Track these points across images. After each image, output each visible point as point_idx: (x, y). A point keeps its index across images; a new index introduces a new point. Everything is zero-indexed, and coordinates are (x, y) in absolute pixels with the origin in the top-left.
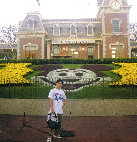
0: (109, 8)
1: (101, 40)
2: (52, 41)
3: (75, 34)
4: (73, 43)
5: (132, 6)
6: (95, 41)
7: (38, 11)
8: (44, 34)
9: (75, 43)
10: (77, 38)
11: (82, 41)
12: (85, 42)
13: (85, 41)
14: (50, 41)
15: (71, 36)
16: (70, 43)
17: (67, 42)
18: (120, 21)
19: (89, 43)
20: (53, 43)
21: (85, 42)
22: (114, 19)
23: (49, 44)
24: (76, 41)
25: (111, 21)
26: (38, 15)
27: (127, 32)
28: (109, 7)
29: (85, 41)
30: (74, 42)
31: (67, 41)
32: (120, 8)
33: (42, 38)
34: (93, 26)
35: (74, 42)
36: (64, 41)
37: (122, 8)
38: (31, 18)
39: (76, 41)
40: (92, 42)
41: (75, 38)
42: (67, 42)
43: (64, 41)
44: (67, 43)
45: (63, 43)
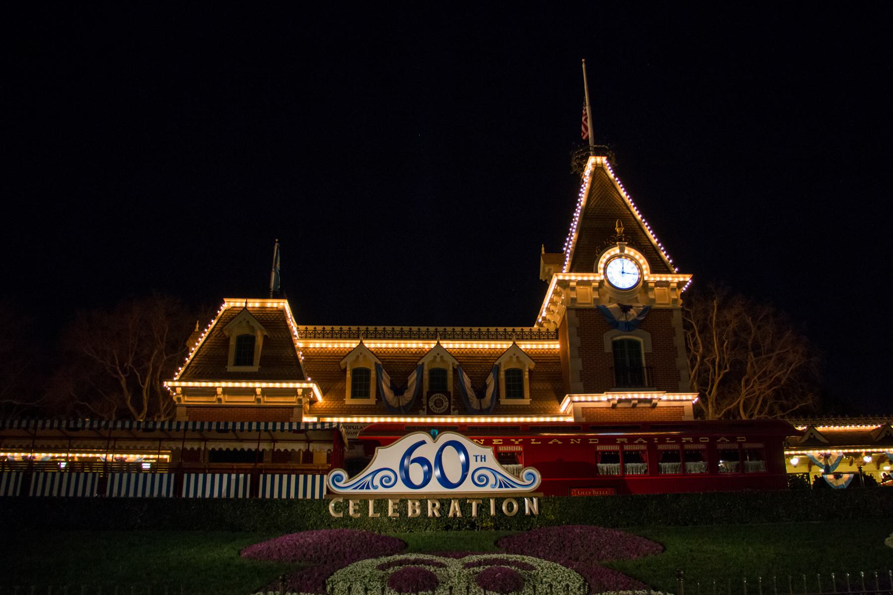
3: (448, 394)
15: (431, 404)
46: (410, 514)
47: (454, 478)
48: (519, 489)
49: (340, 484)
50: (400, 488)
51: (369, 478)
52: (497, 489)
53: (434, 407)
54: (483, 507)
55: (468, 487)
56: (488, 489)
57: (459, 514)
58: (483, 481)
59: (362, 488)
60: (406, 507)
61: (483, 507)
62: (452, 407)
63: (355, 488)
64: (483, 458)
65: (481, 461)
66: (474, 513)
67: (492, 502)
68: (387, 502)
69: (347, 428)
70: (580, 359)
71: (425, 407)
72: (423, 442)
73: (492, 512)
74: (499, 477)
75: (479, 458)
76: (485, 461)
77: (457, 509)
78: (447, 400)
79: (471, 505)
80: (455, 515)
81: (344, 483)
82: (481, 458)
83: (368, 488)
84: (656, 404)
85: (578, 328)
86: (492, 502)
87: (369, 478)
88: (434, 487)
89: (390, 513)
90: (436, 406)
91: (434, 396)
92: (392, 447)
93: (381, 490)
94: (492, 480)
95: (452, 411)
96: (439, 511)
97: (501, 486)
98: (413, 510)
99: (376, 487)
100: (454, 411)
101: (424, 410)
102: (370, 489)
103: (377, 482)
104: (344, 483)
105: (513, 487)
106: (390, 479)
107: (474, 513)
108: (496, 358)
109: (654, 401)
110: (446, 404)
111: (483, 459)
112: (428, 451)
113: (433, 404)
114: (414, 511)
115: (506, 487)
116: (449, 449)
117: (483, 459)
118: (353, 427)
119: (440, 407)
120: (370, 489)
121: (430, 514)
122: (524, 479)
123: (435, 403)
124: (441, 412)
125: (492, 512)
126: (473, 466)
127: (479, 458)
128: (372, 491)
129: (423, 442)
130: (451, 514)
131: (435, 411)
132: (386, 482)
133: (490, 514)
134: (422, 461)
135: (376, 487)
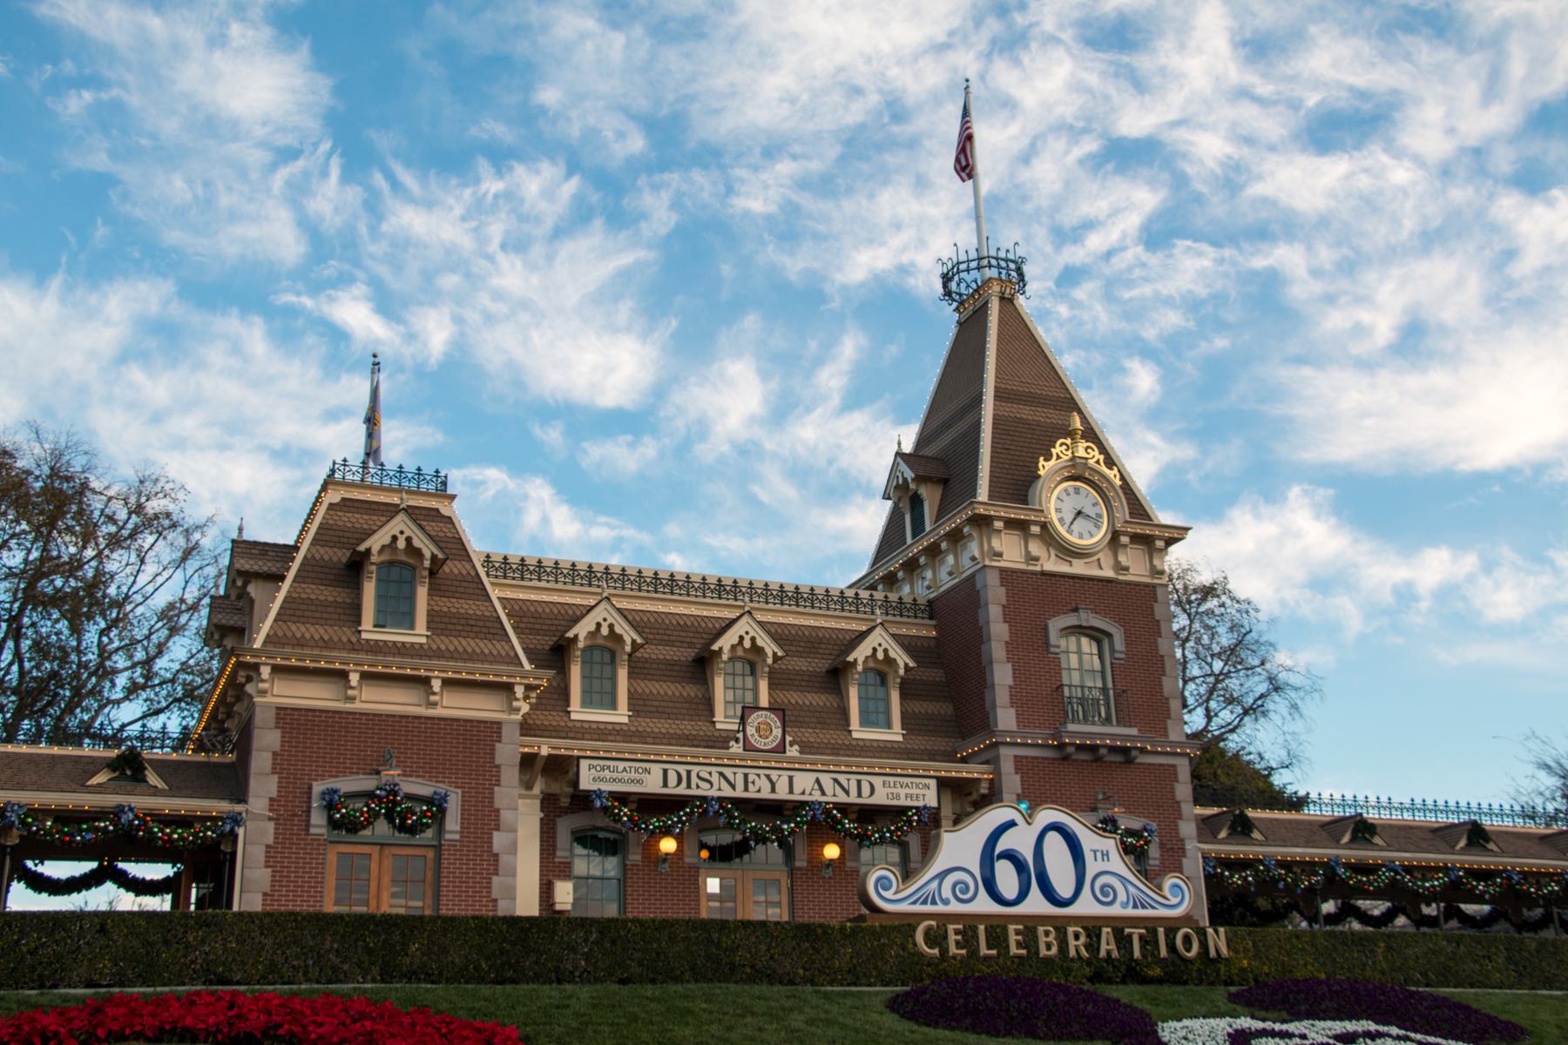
0: (1035, 529)
1: (978, 780)
2: (584, 764)
4: (766, 794)
5: (1187, 529)
6: (933, 783)
7: (442, 474)
8: (529, 688)
9: (782, 793)
10: (793, 751)
11: (836, 780)
12: (860, 795)
13: (859, 782)
14: (561, 767)
15: (750, 730)
16: (739, 793)
17: (715, 778)
18: (1109, 635)
19: (895, 802)
20: (589, 778)
21: (860, 795)
22: (1071, 620)
23: (537, 790)
24: (791, 778)
25: (1056, 625)
26: (444, 511)
27: (1166, 728)
28: (1036, 523)
29: (859, 782)
30: (773, 790)
31: (714, 769)
32: (1109, 536)
33: (499, 723)
34: (902, 658)
35: (773, 790)
36: (689, 772)
37: (1125, 540)
38: (399, 525)
39: (791, 778)
40: (914, 791)
41: (781, 748)
42: (715, 778)
43: (689, 772)
44: (714, 793)
45: (682, 790)
46: (1043, 952)
47: (1064, 890)
48: (1162, 912)
49: (888, 894)
50: (984, 904)
51: (934, 885)
52: (1130, 912)
53: (756, 736)
54: (1149, 941)
55: (1086, 906)
56: (1116, 910)
57: (1115, 954)
58: (1106, 894)
59: (925, 902)
60: (1035, 938)
61: (1147, 942)
62: (788, 738)
63: (914, 903)
64: (1105, 855)
65: (1103, 860)
66: (1137, 954)
67: (1161, 930)
68: (1005, 929)
69: (598, 768)
70: (1010, 665)
71: (740, 735)
72: (1011, 824)
73: (1163, 952)
74: (1131, 889)
75: (1099, 854)
76: (1108, 860)
77: (1113, 946)
78: (779, 724)
79: (1130, 936)
80: (1109, 952)
81: (896, 893)
82: (1103, 855)
83: (934, 902)
84: (1135, 758)
85: (1004, 606)
86: (1161, 930)
87: (934, 885)
88: (1036, 904)
89: (1014, 950)
90: (760, 736)
91: (755, 715)
92: (964, 830)
93: (955, 907)
94: (1122, 896)
95: (788, 747)
96: (1087, 946)
97: (1135, 906)
98: (1047, 946)
99: (946, 902)
100: (791, 746)
101: (737, 740)
102: (936, 904)
103: (946, 892)
104: (896, 893)
105: (1153, 908)
106: (967, 888)
107: (1137, 954)
108: (843, 648)
109: (1134, 753)
110: (778, 732)
111: (1105, 858)
112: (1020, 840)
113: (754, 731)
114: (1049, 947)
115: (1144, 907)
116: (1053, 839)
117: (1105, 858)
118: (609, 767)
119: (767, 738)
120: (936, 904)
121: (1072, 953)
122: (1169, 896)
123: (758, 730)
124: (769, 747)
125: (1163, 952)
126: (1092, 867)
127: (1099, 854)
128: (940, 908)
129: (1011, 824)
130: (1103, 953)
131: (758, 746)
132: (962, 893)
133: (1159, 954)
134: (1010, 856)
135: (946, 902)
